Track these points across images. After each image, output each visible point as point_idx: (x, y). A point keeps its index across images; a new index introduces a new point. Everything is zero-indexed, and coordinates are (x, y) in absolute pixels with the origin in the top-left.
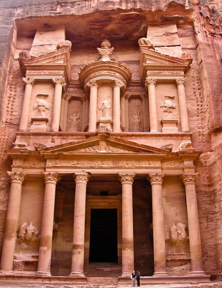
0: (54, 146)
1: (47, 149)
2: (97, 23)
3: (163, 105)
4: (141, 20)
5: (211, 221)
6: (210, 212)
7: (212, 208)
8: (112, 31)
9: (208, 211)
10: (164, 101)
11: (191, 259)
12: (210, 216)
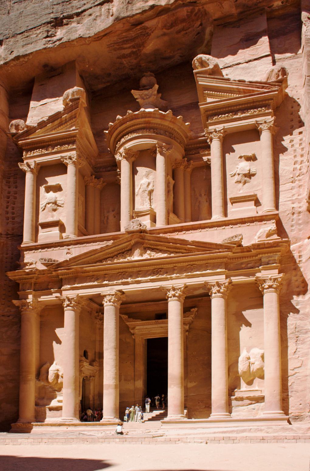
0: (68, 260)
1: (59, 265)
2: (126, 44)
3: (233, 172)
4: (200, 20)
5: (302, 344)
6: (302, 331)
7: (306, 325)
8: (156, 52)
9: (299, 329)
10: (237, 164)
11: (264, 396)
12: (302, 336)
